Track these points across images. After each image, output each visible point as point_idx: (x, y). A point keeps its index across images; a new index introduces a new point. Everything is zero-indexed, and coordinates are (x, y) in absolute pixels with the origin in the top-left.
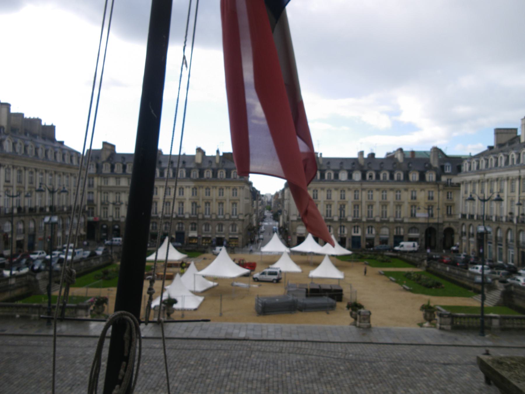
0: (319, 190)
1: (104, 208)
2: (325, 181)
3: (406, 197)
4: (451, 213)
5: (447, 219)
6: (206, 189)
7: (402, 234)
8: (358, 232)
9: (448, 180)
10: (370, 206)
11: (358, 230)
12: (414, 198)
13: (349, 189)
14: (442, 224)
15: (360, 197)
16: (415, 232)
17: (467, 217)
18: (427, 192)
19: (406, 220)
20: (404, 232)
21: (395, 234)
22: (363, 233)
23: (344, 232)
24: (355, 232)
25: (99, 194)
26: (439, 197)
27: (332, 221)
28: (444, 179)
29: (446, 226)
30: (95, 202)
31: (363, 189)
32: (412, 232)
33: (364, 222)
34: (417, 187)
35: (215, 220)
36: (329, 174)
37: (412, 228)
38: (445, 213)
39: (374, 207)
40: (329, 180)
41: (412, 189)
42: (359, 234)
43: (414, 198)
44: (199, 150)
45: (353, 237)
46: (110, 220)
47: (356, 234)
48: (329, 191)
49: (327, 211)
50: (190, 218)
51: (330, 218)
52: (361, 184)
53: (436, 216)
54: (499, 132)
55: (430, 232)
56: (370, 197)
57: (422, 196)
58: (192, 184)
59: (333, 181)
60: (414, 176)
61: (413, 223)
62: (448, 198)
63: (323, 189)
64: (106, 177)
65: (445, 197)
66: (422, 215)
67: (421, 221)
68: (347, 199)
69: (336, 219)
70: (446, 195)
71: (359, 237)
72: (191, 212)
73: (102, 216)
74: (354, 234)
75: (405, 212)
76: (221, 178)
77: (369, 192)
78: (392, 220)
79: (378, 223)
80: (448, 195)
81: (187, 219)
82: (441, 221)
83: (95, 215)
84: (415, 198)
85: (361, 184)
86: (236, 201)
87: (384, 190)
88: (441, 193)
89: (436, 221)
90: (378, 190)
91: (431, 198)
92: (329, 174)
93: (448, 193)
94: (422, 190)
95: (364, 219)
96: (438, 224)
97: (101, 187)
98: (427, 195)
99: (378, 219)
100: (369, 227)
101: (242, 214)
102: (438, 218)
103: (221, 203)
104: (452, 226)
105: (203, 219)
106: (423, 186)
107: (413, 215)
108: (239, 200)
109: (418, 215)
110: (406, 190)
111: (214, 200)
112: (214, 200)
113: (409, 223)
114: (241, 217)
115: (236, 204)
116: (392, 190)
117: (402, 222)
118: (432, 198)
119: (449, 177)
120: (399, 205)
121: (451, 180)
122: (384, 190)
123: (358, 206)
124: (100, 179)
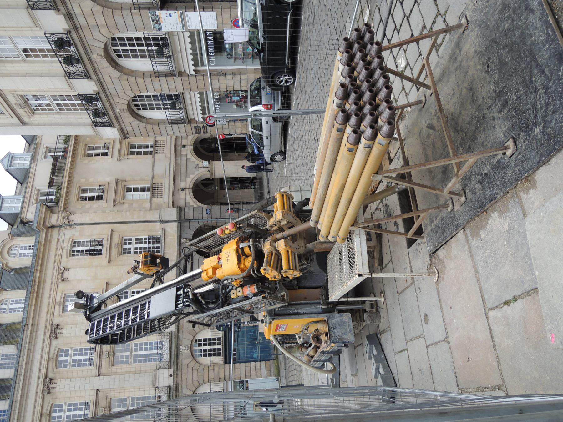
5: (166, 197)
14: (180, 210)
21: (220, 359)
29: (188, 198)
65: (96, 204)
70: (88, 203)
80: (91, 199)
82: (173, 214)
88: (76, 218)
89: (172, 229)
96: (181, 221)
98: (86, 259)
102: (162, 222)
104: (188, 182)
106: (51, 273)
116: (48, 385)
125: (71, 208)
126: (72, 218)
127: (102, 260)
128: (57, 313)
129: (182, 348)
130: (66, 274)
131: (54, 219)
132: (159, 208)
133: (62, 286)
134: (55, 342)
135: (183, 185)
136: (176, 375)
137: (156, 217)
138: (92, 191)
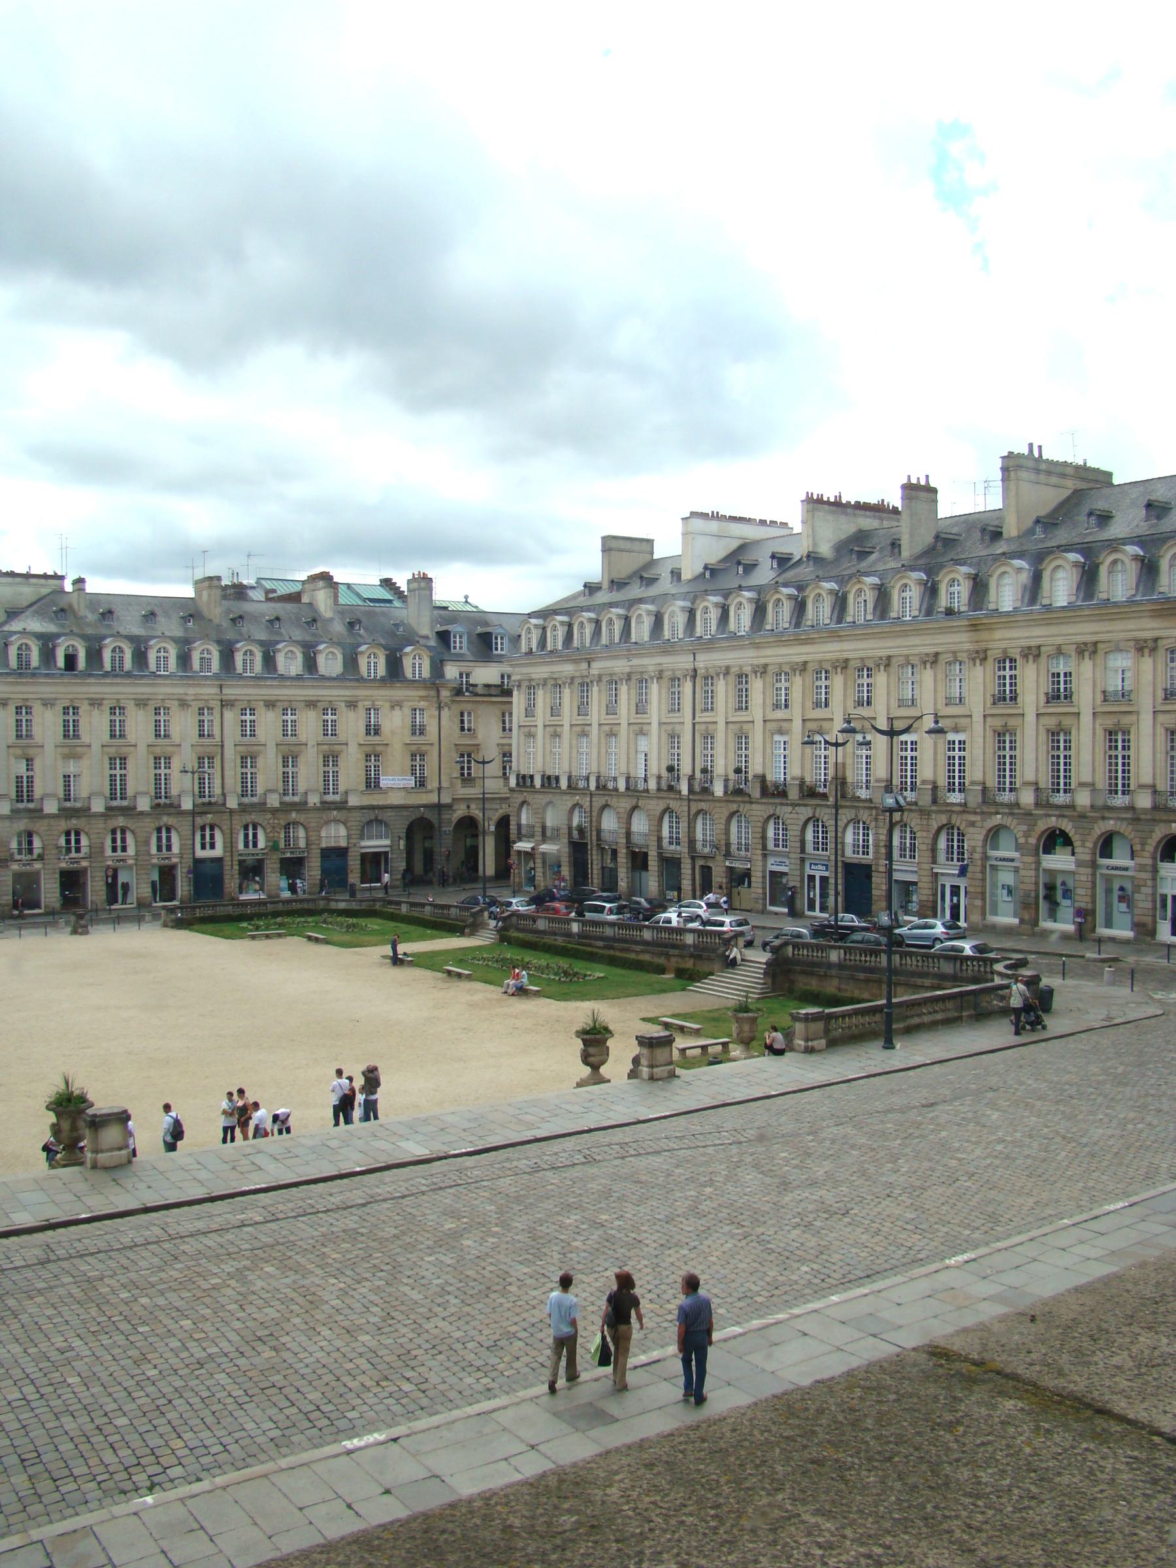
0: (84, 708)
2: (106, 675)
3: (352, 725)
4: (469, 774)
7: (343, 844)
8: (213, 846)
9: (461, 675)
10: (248, 758)
11: (212, 837)
12: (373, 730)
13: (184, 704)
14: (449, 807)
15: (217, 731)
16: (379, 837)
17: (538, 782)
18: (407, 711)
19: (353, 801)
20: (349, 837)
21: (324, 845)
22: (230, 845)
23: (169, 848)
24: (203, 847)
26: (442, 726)
27: (129, 811)
28: (451, 671)
29: (460, 812)
31: (225, 704)
32: (370, 838)
33: (231, 811)
34: (382, 696)
36: (117, 650)
37: (370, 822)
38: (457, 774)
39: (260, 762)
40: (117, 672)
41: (368, 704)
42: (218, 852)
43: (373, 730)
45: (198, 862)
47: (208, 853)
48: (117, 709)
49: (112, 778)
51: (125, 803)
52: (221, 687)
53: (432, 784)
54: (611, 546)
55: (421, 828)
56: (248, 730)
57: (395, 723)
59: (128, 675)
60: (373, 663)
61: (372, 808)
62: (462, 729)
63: (95, 703)
65: (456, 727)
66: (396, 781)
67: (395, 799)
68: (131, 737)
69: (144, 804)
70: (457, 720)
71: (219, 860)
74: (200, 854)
75: (350, 773)
77: (243, 712)
78: (314, 800)
79: (274, 811)
80: (462, 722)
82: (446, 799)
84: (377, 733)
85: (221, 687)
87: (289, 708)
88: (445, 713)
89: (433, 799)
90: (270, 704)
91: (418, 730)
92: (117, 650)
93: (462, 714)
94: (396, 704)
95: (232, 803)
96: (439, 807)
98: (409, 721)
99: (274, 801)
100: (246, 828)
102: (439, 789)
104: (476, 812)
106: (398, 693)
107: (372, 784)
109: (385, 782)
110: (352, 705)
113: (362, 808)
116: (311, 704)
117: (342, 806)
118: (422, 732)
119: (465, 667)
120: (331, 758)
121: (468, 675)
122: (289, 708)
123: (211, 758)
125: (453, 707)
126: (446, 709)
127: (408, 732)
128: (366, 703)
129: (335, 813)
130: (397, 708)
131: (445, 693)
132: (452, 785)
133: (388, 705)
134: (343, 704)
135: (473, 806)
136: (315, 809)
137: (444, 784)
138: (469, 722)
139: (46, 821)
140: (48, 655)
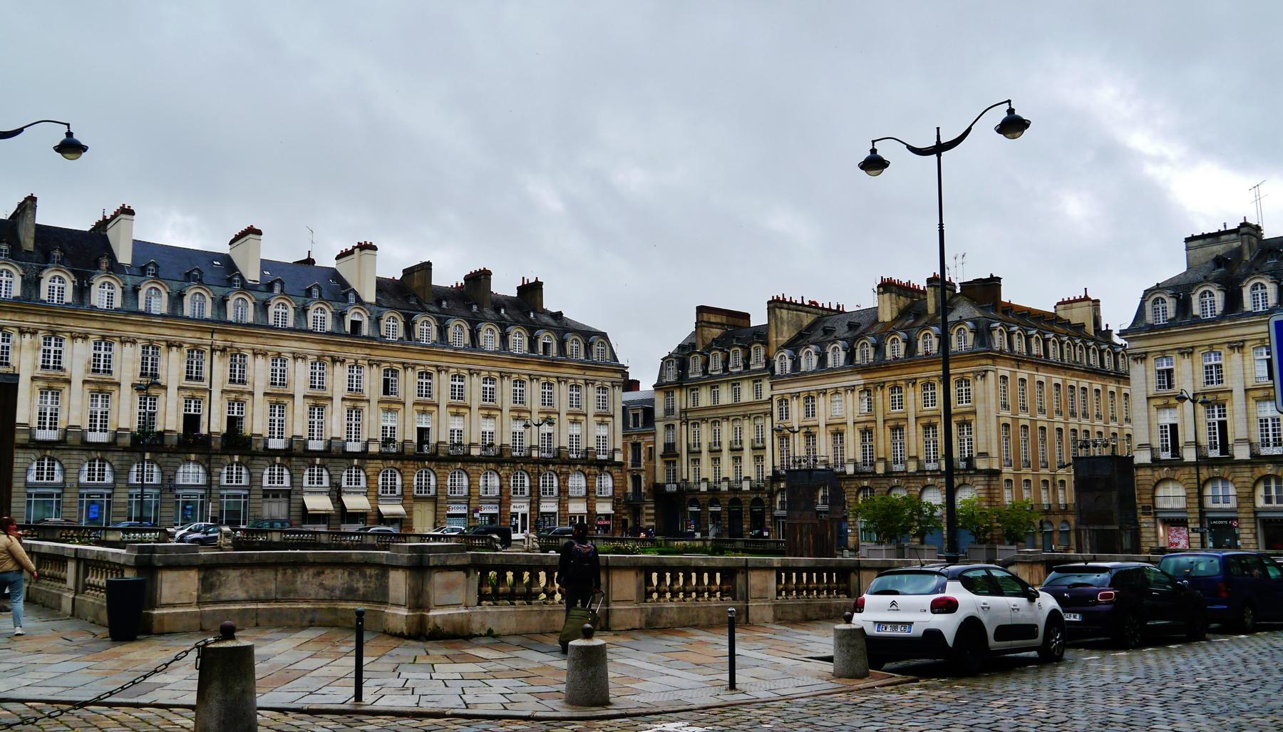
1: (694, 460)
6: (892, 389)
25: (684, 427)
30: (677, 447)
35: (913, 476)
44: (887, 286)
46: (704, 488)
50: (859, 474)
58: (858, 380)
64: (694, 387)
72: (859, 459)
73: (691, 480)
76: (896, 358)
81: (850, 477)
83: (678, 480)
86: (968, 418)
97: (685, 411)
101: (984, 455)
103: (897, 429)
105: (889, 474)
108: (975, 413)
111: (912, 420)
112: (912, 420)
114: (981, 464)
115: (969, 424)
124: (684, 393)
139: (1187, 470)
140: (1184, 306)
